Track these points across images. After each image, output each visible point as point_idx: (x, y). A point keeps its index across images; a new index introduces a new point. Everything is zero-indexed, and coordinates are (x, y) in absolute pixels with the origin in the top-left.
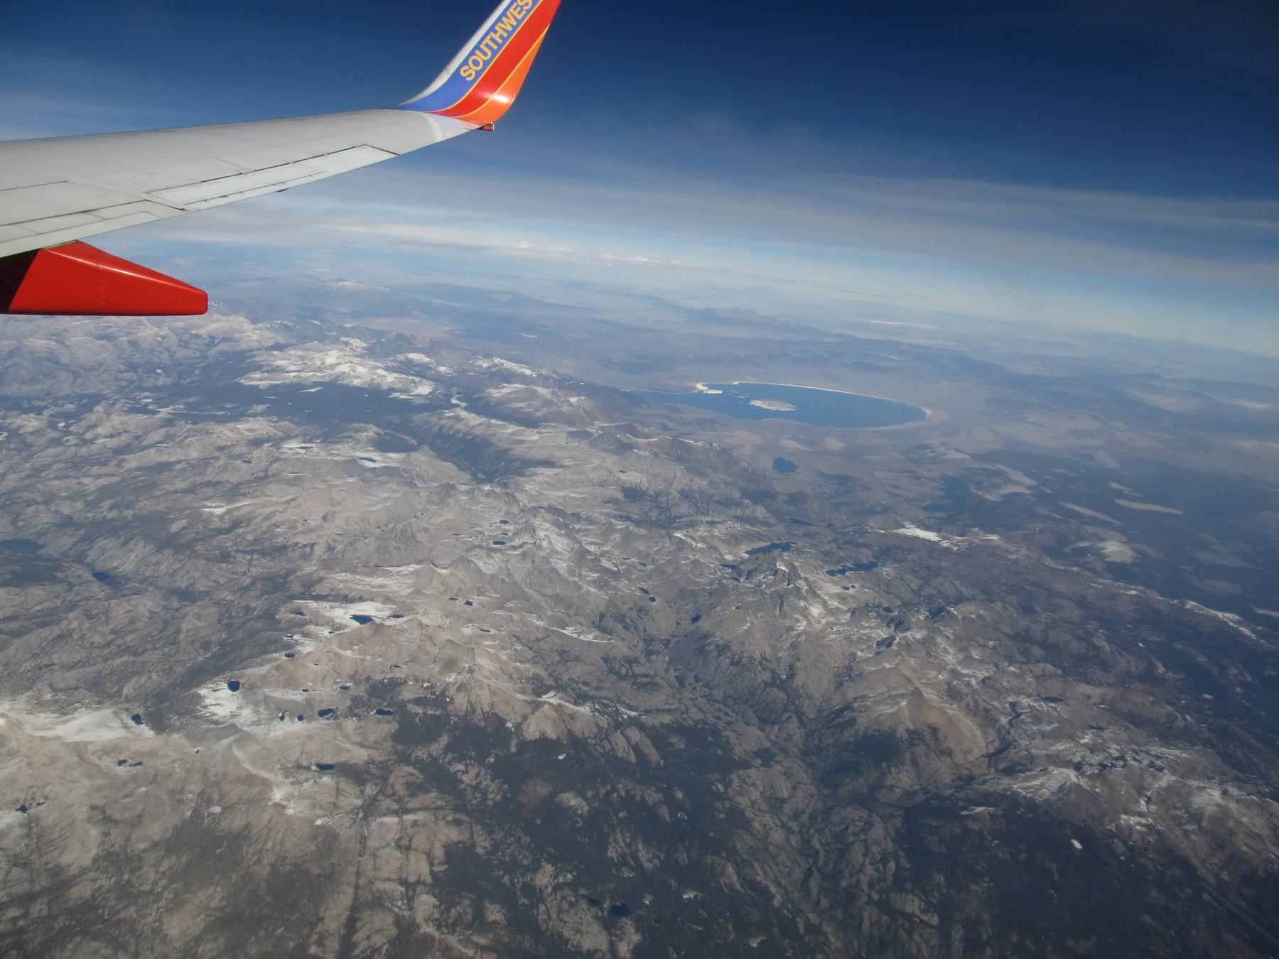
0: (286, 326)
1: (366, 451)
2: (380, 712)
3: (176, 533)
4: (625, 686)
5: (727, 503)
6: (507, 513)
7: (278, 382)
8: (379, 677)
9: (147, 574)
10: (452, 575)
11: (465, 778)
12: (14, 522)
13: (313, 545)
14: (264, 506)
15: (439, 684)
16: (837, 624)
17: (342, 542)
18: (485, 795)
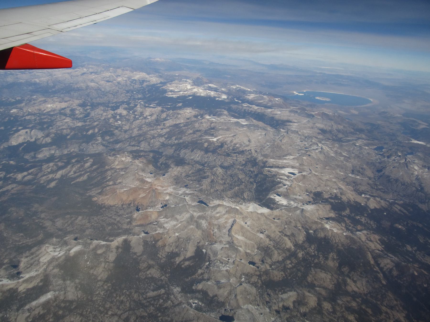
0: (160, 76)
1: (232, 119)
2: (322, 202)
3: (207, 148)
4: (379, 192)
5: (351, 133)
6: (301, 138)
7: (179, 95)
8: (313, 191)
9: (206, 161)
10: (307, 159)
11: (362, 220)
12: (149, 145)
13: (251, 150)
14: (226, 138)
15: (332, 193)
16: (424, 172)
17: (258, 149)
18: (371, 225)
